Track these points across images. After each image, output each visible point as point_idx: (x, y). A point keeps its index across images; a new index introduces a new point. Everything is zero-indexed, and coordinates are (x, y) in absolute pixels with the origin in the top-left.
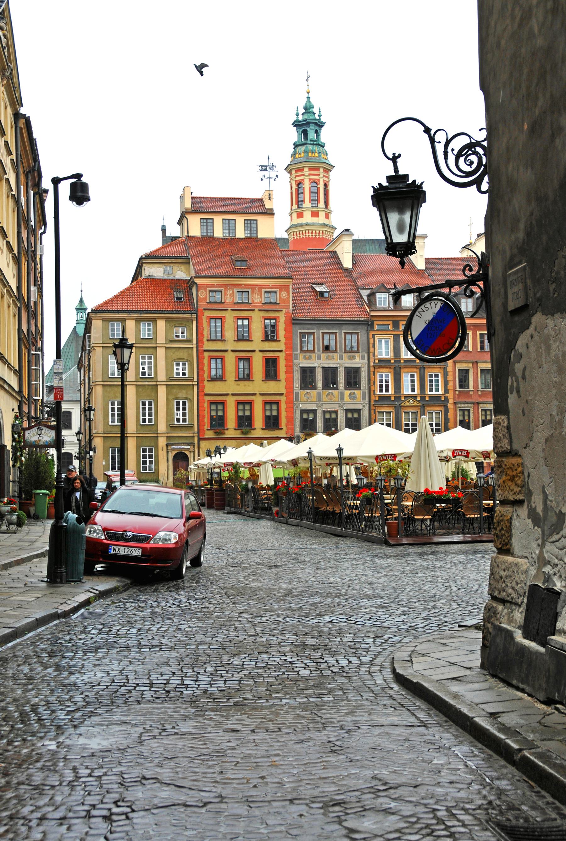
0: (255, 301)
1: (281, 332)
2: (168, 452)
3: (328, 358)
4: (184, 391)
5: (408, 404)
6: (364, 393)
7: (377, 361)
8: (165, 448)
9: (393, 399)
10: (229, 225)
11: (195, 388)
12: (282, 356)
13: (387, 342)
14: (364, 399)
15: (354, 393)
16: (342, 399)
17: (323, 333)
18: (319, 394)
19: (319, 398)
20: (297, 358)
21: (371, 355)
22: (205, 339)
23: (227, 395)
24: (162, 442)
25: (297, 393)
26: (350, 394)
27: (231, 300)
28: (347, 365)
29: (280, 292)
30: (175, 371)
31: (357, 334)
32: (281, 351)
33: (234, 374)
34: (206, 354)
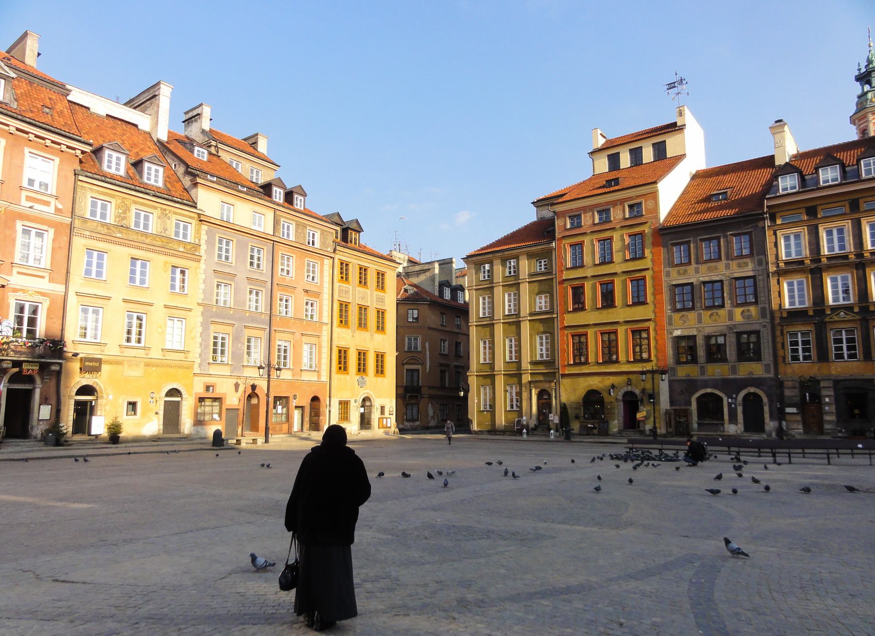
3: (710, 269)
5: (836, 319)
6: (763, 310)
7: (782, 265)
9: (811, 313)
10: (636, 154)
12: (648, 275)
13: (797, 236)
16: (731, 316)
18: (700, 316)
19: (700, 321)
20: (668, 274)
21: (771, 258)
26: (743, 312)
28: (736, 275)
29: (646, 201)
30: (538, 304)
31: (749, 233)
32: (647, 269)
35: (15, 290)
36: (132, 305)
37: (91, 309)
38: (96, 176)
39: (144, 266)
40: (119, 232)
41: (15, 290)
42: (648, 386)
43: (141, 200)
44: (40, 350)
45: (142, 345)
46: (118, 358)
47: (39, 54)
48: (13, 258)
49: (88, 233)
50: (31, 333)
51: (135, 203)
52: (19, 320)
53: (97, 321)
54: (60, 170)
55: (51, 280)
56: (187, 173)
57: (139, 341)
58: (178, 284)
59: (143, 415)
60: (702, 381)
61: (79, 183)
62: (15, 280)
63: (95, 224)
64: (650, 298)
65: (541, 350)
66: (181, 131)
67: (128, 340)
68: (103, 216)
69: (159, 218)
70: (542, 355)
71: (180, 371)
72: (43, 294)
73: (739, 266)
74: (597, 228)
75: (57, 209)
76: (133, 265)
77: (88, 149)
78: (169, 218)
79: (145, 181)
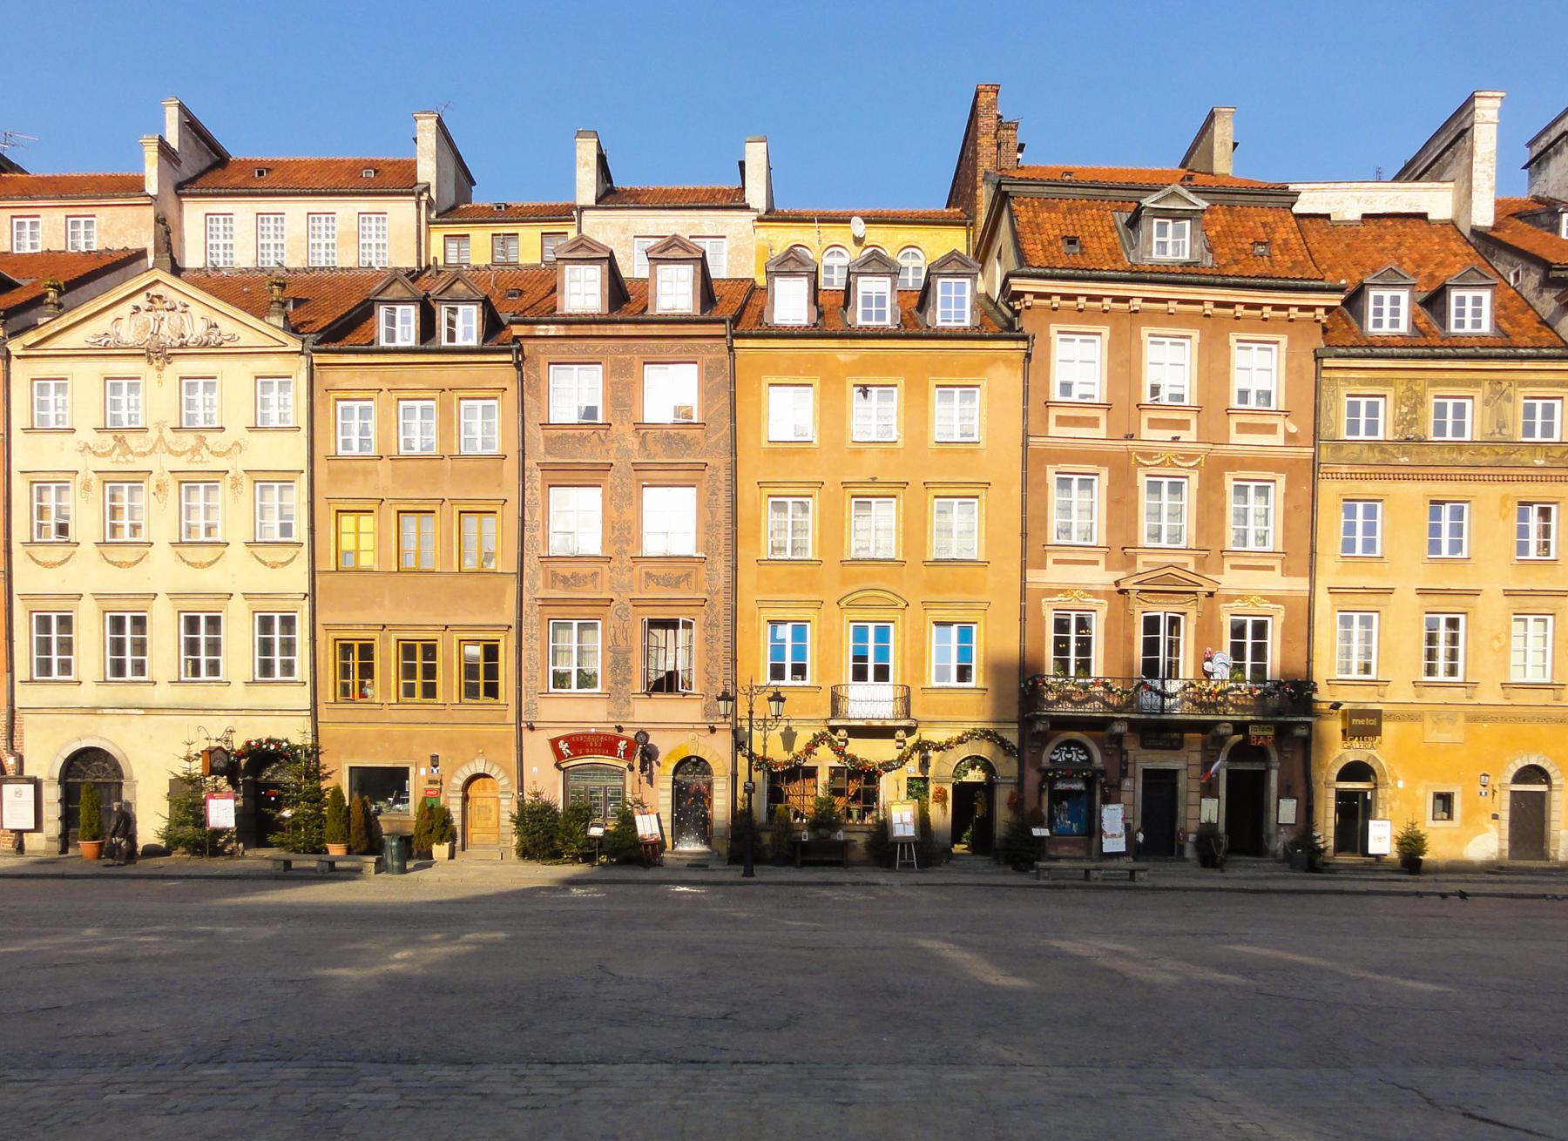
35: (1229, 599)
36: (1435, 600)
37: (1356, 616)
38: (1353, 351)
39: (1458, 514)
40: (1405, 453)
41: (1229, 599)
43: (1447, 375)
44: (1273, 702)
45: (1459, 678)
46: (1412, 708)
47: (1235, 145)
48: (1223, 542)
49: (1344, 469)
50: (1259, 671)
51: (1434, 383)
52: (1238, 651)
53: (1368, 638)
54: (1290, 358)
55: (1286, 572)
56: (1547, 283)
57: (1452, 671)
58: (1533, 539)
59: (1466, 819)
61: (1325, 374)
62: (1229, 580)
63: (1356, 449)
66: (1522, 192)
67: (1431, 671)
68: (1372, 427)
69: (1486, 402)
71: (1544, 729)
72: (1273, 599)
75: (1290, 438)
76: (1435, 515)
77: (1335, 300)
78: (1509, 399)
79: (1453, 329)
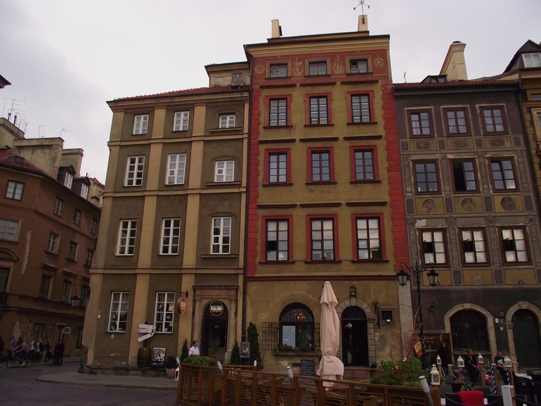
0: (336, 72)
1: (379, 113)
2: (194, 301)
3: (458, 145)
4: (226, 203)
6: (527, 199)
8: (191, 294)
11: (244, 197)
12: (381, 145)
14: (529, 207)
15: (510, 199)
17: (446, 110)
20: (405, 147)
21: (531, 137)
22: (261, 127)
23: (294, 206)
24: (187, 283)
25: (410, 202)
26: (503, 201)
27: (300, 74)
29: (373, 59)
33: (304, 175)
34: (262, 148)
42: (381, 299)
60: (457, 292)
64: (383, 174)
65: (216, 240)
70: (216, 248)
73: (494, 144)
74: (308, 81)
